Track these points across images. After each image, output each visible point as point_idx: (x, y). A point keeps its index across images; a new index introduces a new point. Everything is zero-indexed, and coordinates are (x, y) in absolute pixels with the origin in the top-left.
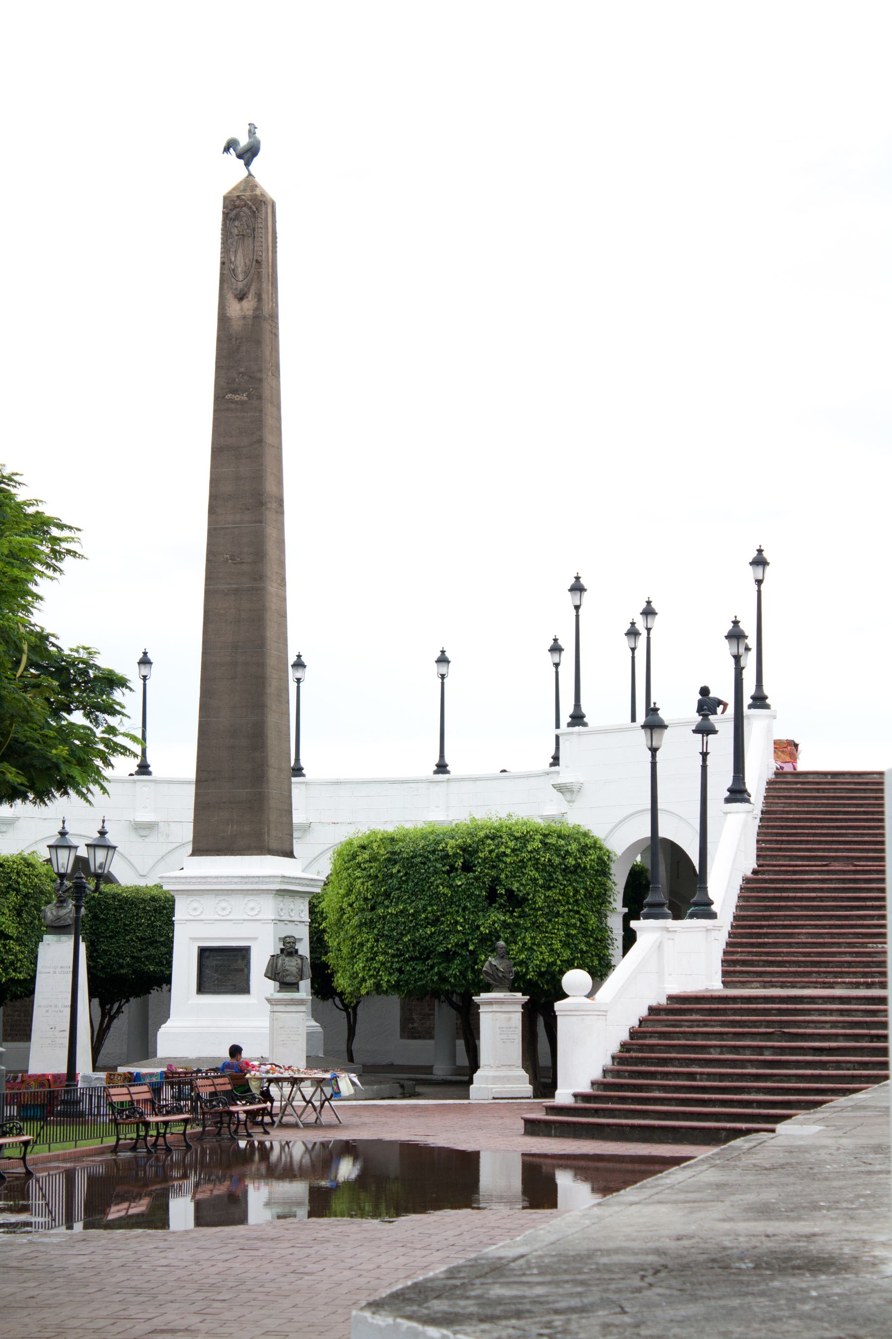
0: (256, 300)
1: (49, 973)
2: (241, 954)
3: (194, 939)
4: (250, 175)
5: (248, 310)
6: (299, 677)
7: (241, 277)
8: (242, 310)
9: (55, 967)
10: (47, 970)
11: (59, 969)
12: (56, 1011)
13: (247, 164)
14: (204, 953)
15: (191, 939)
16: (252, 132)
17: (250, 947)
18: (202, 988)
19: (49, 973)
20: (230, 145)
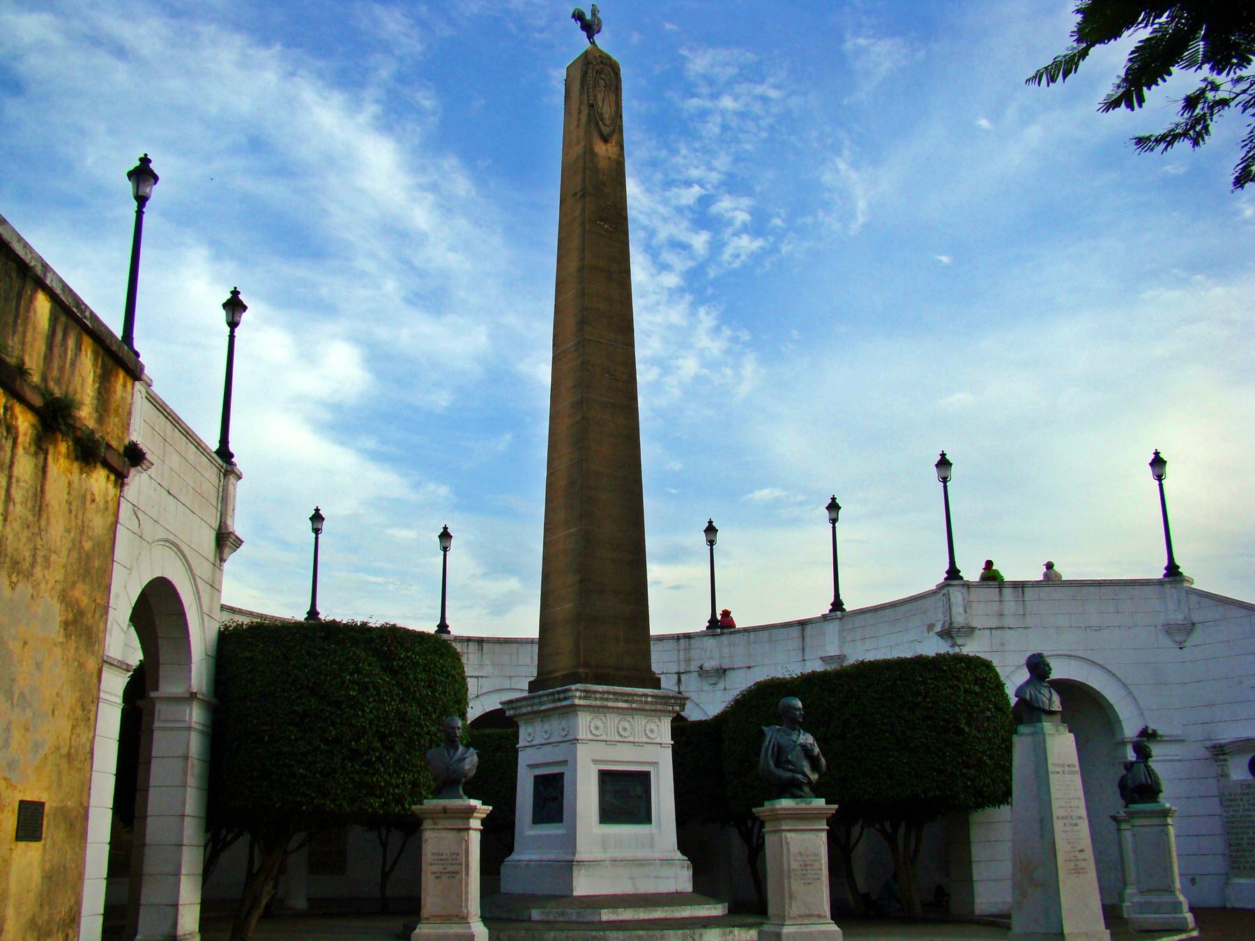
0: (619, 148)
1: (1058, 773)
2: (643, 779)
3: (595, 761)
4: (593, 43)
5: (612, 153)
6: (315, 527)
7: (608, 122)
8: (607, 150)
9: (1063, 766)
10: (1058, 769)
11: (1067, 769)
12: (1072, 825)
13: (590, 37)
14: (605, 776)
15: (593, 760)
16: (594, 14)
17: (649, 772)
18: (609, 814)
19: (1058, 773)
20: (578, 16)
